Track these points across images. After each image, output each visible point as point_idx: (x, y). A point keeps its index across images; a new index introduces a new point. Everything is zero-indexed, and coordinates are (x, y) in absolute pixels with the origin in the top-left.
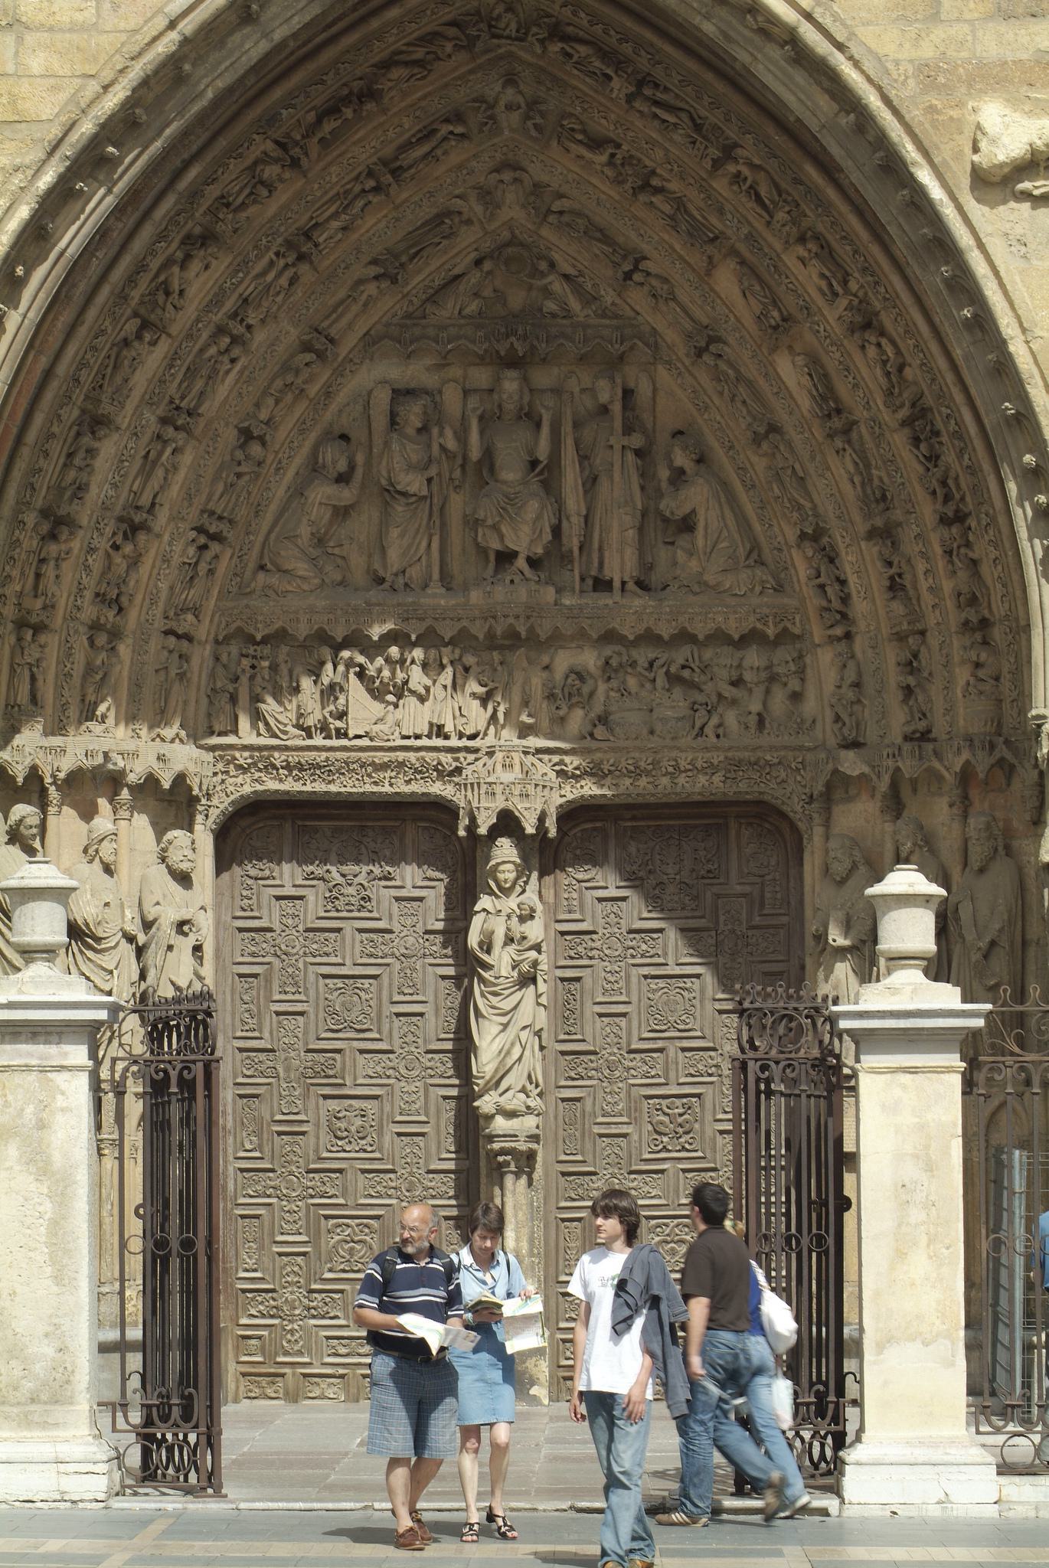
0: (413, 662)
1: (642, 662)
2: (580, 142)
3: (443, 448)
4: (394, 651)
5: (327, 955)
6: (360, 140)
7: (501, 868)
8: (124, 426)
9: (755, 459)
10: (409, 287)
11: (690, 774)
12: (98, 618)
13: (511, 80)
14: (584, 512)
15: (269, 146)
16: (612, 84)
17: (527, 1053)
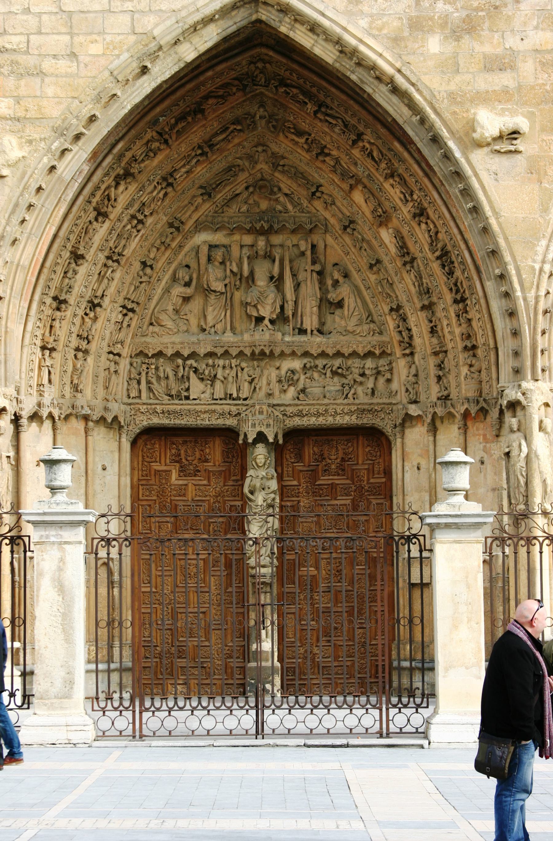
0: (219, 366)
1: (320, 366)
2: (293, 133)
3: (231, 271)
5: (180, 496)
6: (195, 132)
7: (258, 457)
9: (370, 276)
13: (262, 105)
14: (294, 299)
15: (154, 134)
16: (308, 106)
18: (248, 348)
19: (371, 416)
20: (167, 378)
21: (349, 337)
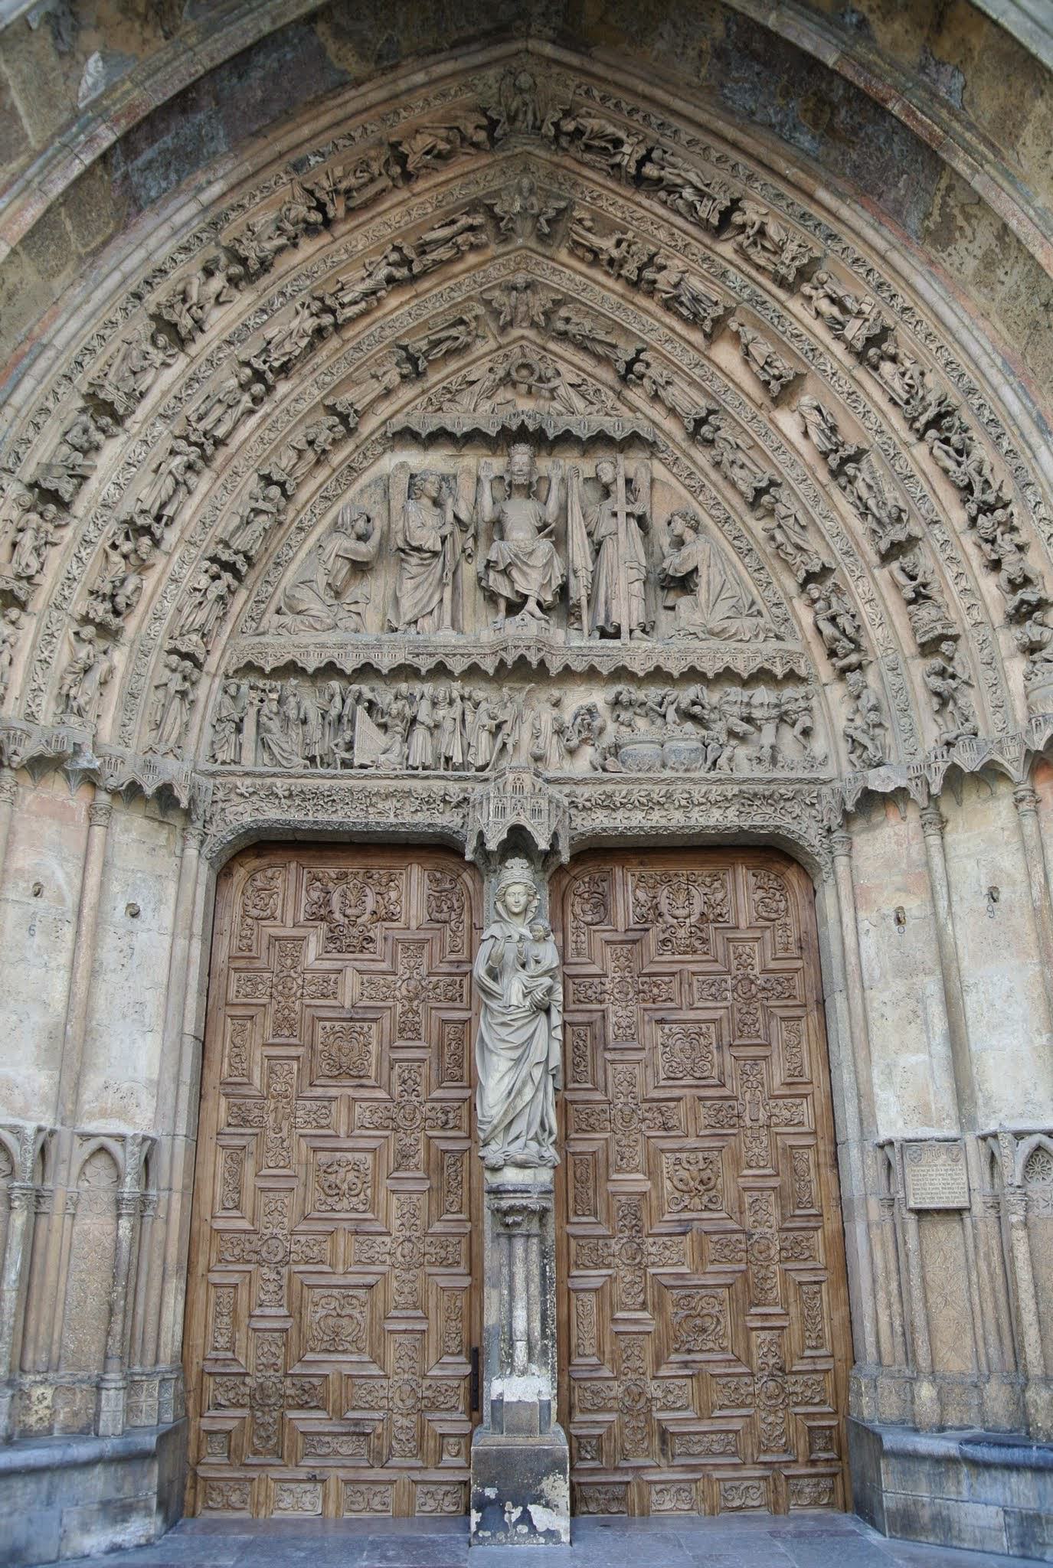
2: (589, 230)
3: (456, 517)
4: (403, 687)
7: (511, 889)
8: (133, 431)
11: (703, 807)
15: (298, 191)
17: (541, 1095)
19: (770, 810)
20: (304, 722)
21: (714, 643)
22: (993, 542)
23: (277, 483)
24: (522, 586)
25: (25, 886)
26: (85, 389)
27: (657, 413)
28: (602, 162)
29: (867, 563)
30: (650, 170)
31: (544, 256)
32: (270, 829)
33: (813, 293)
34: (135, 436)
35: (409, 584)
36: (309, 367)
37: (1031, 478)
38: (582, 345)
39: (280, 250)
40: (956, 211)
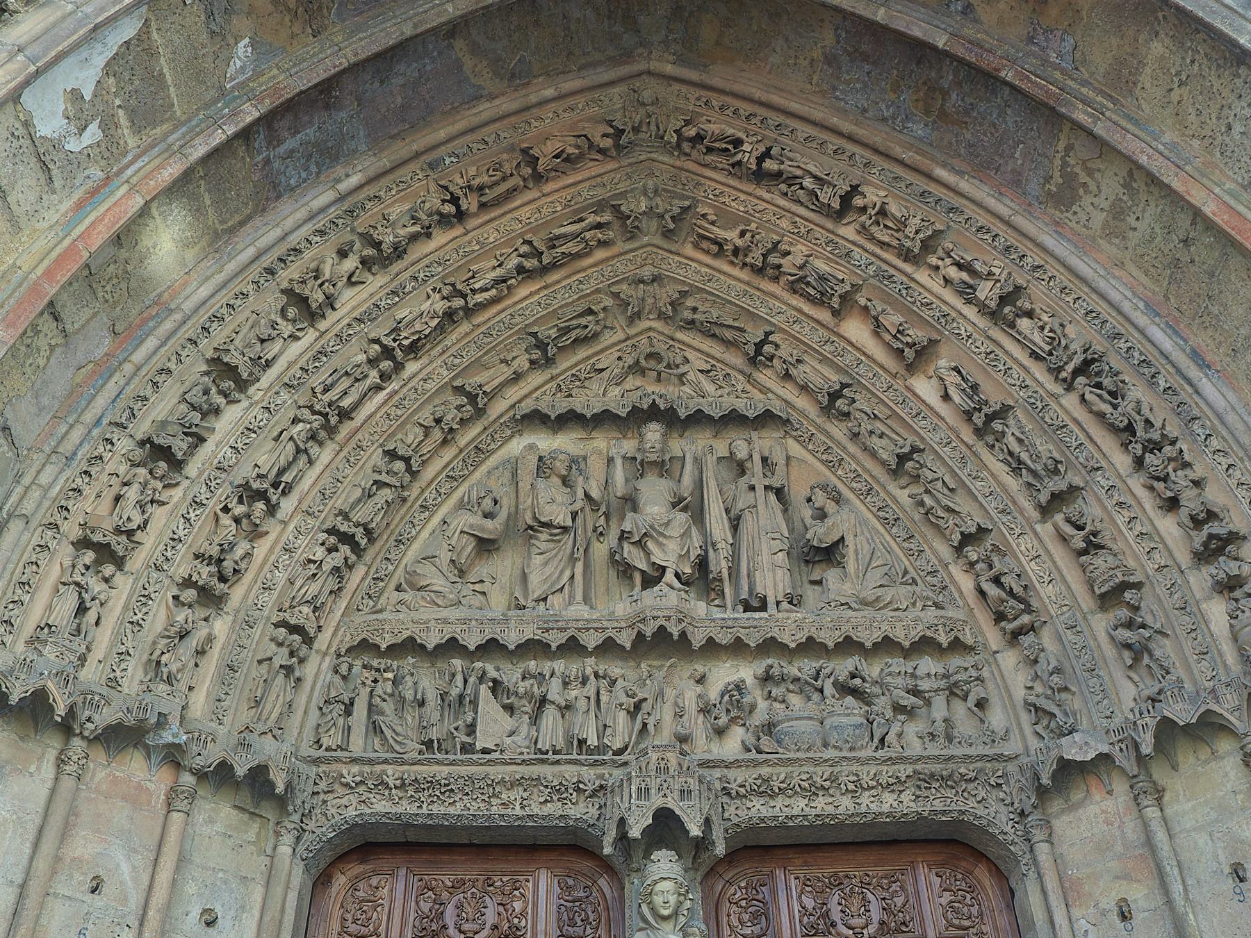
2: (713, 223)
3: (586, 495)
4: (532, 664)
7: (659, 887)
10: (558, 371)
11: (874, 792)
12: (190, 576)
15: (432, 186)
18: (624, 633)
20: (422, 704)
21: (868, 612)
22: (1165, 479)
23: (402, 458)
24: (658, 558)
25: (82, 880)
26: (210, 354)
27: (789, 392)
28: (723, 162)
29: (1027, 520)
30: (769, 165)
31: (671, 252)
32: (378, 824)
33: (940, 263)
34: (257, 403)
35: (538, 560)
36: (439, 349)
37: (1196, 412)
38: (710, 331)
39: (414, 238)
40: (1078, 170)
